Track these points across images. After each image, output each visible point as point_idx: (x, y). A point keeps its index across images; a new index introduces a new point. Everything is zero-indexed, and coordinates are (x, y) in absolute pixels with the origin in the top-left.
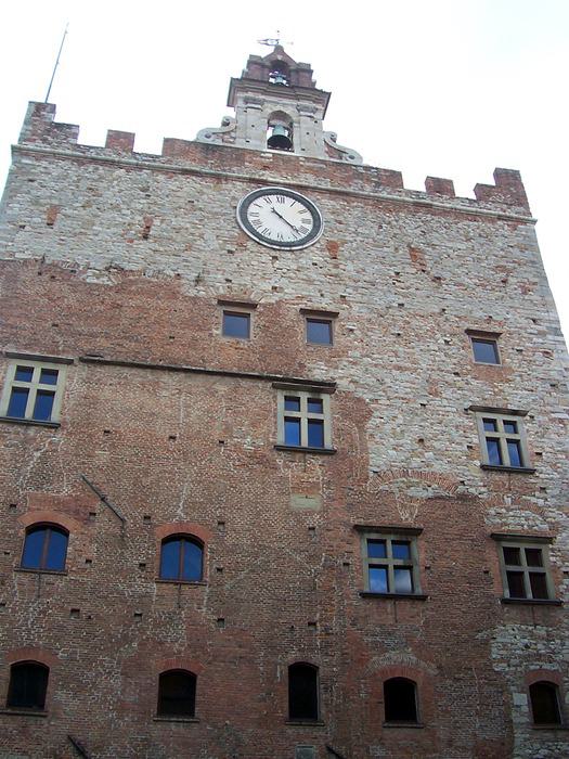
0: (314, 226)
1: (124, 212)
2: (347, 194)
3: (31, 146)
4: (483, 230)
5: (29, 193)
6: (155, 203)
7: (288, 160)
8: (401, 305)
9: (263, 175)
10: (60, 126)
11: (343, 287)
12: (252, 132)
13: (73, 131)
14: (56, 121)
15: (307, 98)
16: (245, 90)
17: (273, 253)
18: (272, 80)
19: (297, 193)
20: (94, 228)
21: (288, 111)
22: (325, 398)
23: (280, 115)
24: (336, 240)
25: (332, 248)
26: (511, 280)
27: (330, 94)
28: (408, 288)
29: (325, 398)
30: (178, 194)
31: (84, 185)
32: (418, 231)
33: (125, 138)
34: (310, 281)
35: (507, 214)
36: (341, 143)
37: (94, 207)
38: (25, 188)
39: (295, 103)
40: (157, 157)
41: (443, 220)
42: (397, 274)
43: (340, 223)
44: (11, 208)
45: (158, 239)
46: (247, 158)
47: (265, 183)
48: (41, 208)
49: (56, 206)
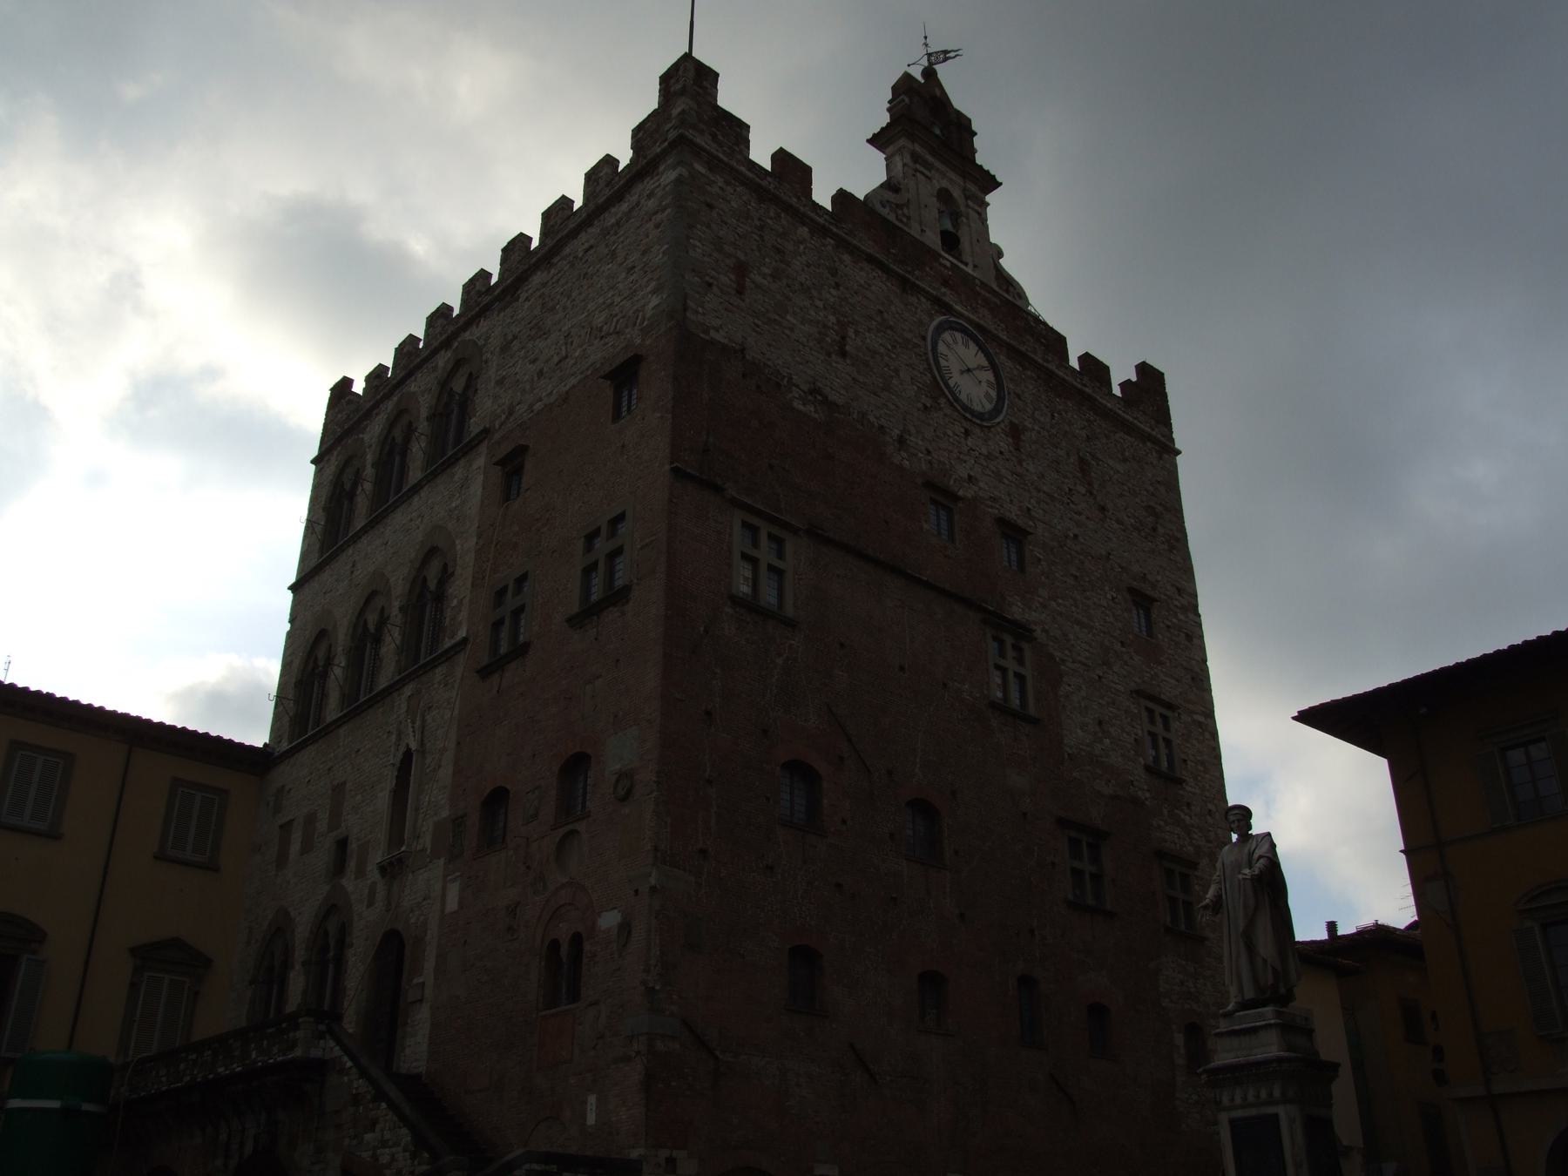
5: (709, 227)
8: (1076, 536)
17: (967, 425)
19: (979, 336)
21: (956, 193)
22: (1025, 645)
25: (1015, 432)
26: (1161, 530)
28: (1080, 514)
29: (1025, 645)
43: (1018, 396)
47: (946, 309)
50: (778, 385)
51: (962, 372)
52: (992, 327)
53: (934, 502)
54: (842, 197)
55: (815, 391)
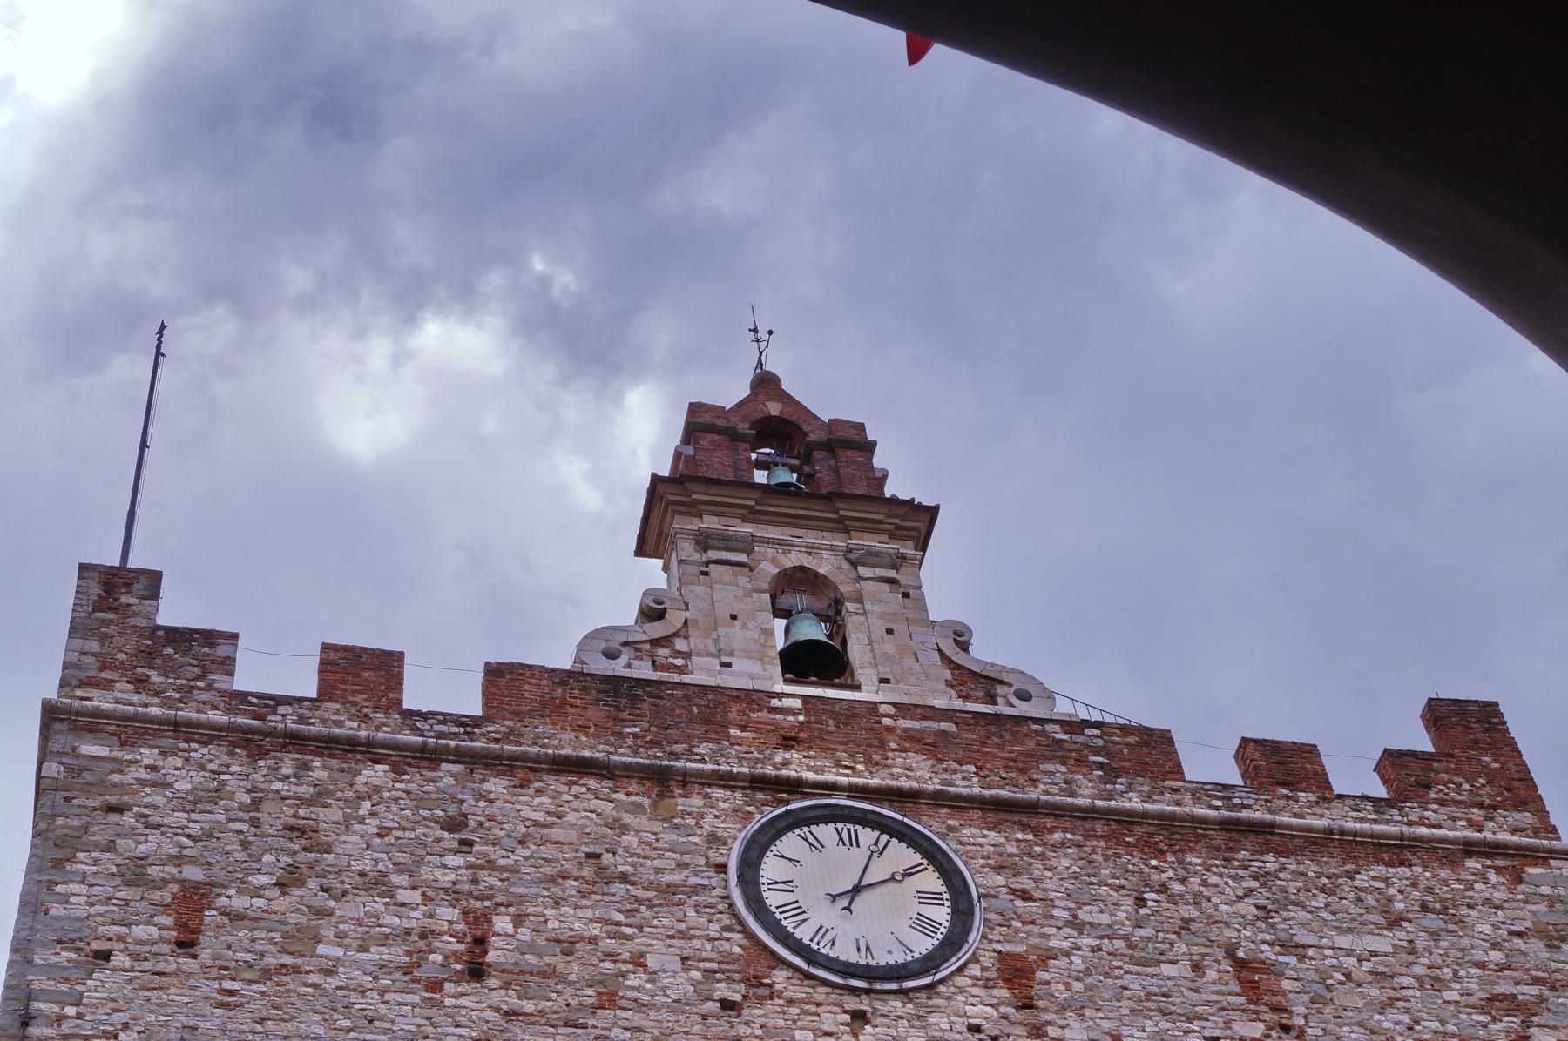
0: (956, 912)
1: (404, 895)
2: (1032, 808)
3: (101, 701)
4: (1429, 890)
5: (110, 847)
6: (491, 865)
7: (848, 714)
10: (181, 637)
12: (736, 635)
13: (222, 650)
14: (162, 620)
15: (870, 527)
16: (694, 509)
17: (852, 1003)
18: (760, 477)
20: (321, 949)
21: (825, 566)
23: (799, 580)
24: (1020, 949)
25: (1016, 974)
27: (933, 511)
30: (556, 833)
31: (274, 816)
32: (1247, 908)
33: (377, 669)
35: (1490, 836)
36: (984, 652)
37: (313, 884)
38: (97, 835)
39: (840, 541)
40: (476, 722)
41: (1312, 868)
43: (1025, 896)
44: (65, 899)
45: (514, 977)
46: (733, 715)
47: (796, 787)
48: (156, 896)
49: (197, 885)
52: (934, 785)
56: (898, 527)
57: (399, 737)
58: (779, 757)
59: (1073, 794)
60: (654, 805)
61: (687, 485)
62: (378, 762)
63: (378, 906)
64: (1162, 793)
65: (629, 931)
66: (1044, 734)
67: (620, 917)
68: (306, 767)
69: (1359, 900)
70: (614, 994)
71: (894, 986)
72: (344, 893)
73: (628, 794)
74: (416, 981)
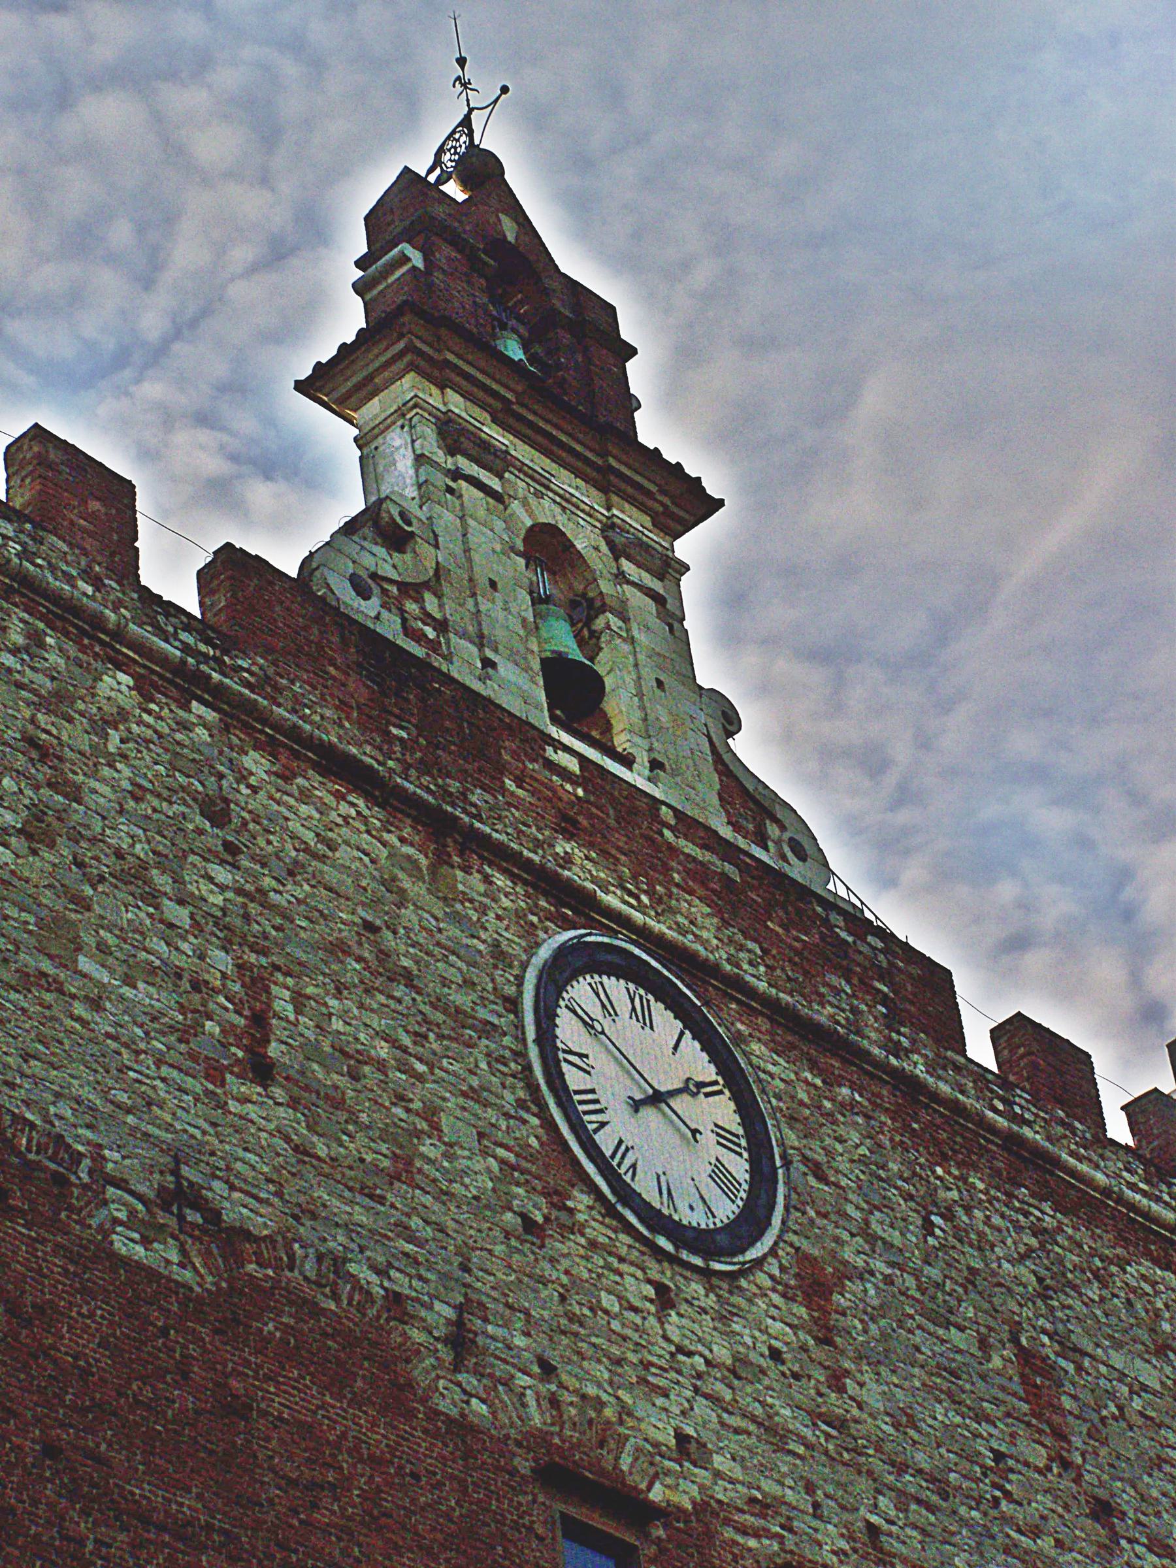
9: (567, 860)
11: (863, 1485)
19: (679, 983)
21: (585, 539)
24: (815, 1252)
25: (814, 1285)
28: (1035, 1532)
34: (776, 1435)
41: (1083, 1235)
42: (999, 1456)
47: (579, 905)
50: (61, 1181)
51: (636, 1106)
53: (576, 1531)
54: (231, 570)
55: (179, 1196)
56: (667, 512)
57: (155, 639)
58: (562, 847)
59: (859, 1033)
60: (433, 869)
61: (443, 331)
62: (119, 667)
63: (142, 914)
64: (944, 1068)
65: (421, 1068)
66: (826, 922)
67: (406, 1040)
68: (36, 639)
69: (1129, 1302)
70: (410, 1163)
71: (698, 1261)
72: (102, 879)
73: (402, 840)
74: (193, 1056)
